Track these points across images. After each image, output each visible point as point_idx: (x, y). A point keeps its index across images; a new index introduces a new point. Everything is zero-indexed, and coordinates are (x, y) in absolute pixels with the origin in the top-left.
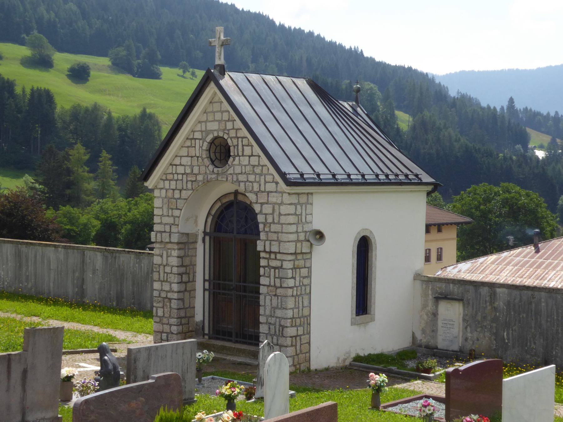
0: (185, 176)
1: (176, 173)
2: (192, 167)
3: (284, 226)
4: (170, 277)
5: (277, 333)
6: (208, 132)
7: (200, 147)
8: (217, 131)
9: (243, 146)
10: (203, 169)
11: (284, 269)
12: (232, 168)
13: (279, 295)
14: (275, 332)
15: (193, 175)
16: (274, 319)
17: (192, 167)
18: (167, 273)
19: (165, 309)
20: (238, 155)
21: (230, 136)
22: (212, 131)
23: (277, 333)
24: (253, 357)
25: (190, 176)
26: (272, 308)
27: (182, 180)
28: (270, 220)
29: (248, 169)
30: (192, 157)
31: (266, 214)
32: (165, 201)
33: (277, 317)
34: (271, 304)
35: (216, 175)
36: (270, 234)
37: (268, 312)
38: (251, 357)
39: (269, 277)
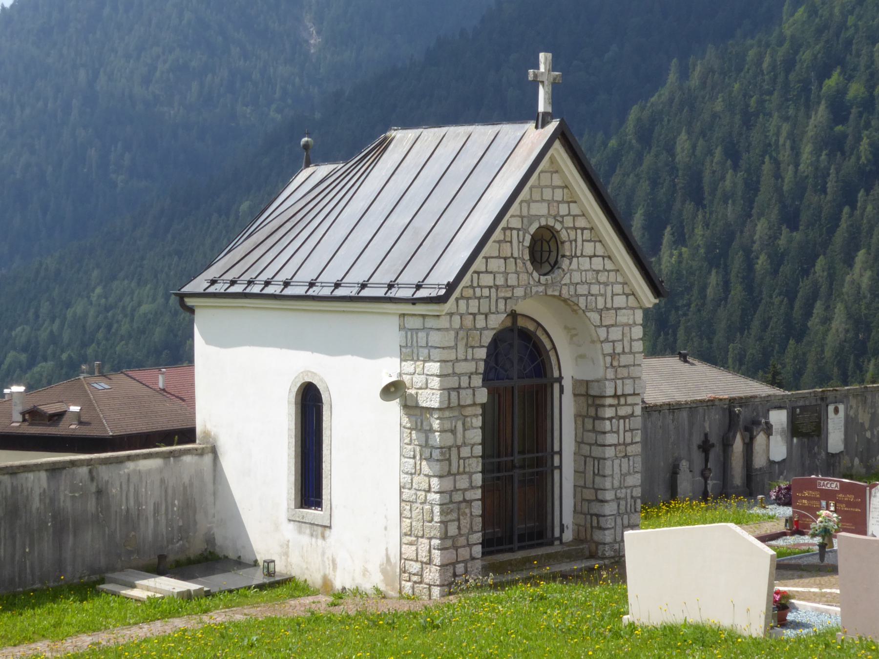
0: (493, 290)
1: (479, 286)
2: (506, 274)
3: (636, 355)
4: (469, 465)
5: (629, 510)
6: (532, 218)
7: (519, 242)
8: (546, 217)
9: (583, 241)
10: (524, 277)
11: (635, 416)
12: (568, 275)
13: (629, 454)
14: (626, 509)
15: (508, 289)
16: (624, 491)
17: (506, 274)
18: (464, 459)
19: (461, 522)
20: (576, 256)
21: (565, 226)
22: (538, 217)
23: (629, 510)
24: (568, 560)
25: (504, 290)
26: (621, 474)
27: (489, 297)
28: (619, 349)
29: (590, 276)
30: (505, 259)
31: (613, 342)
32: (462, 334)
33: (626, 487)
34: (621, 471)
35: (544, 287)
36: (619, 369)
37: (616, 484)
38: (566, 560)
39: (617, 432)
